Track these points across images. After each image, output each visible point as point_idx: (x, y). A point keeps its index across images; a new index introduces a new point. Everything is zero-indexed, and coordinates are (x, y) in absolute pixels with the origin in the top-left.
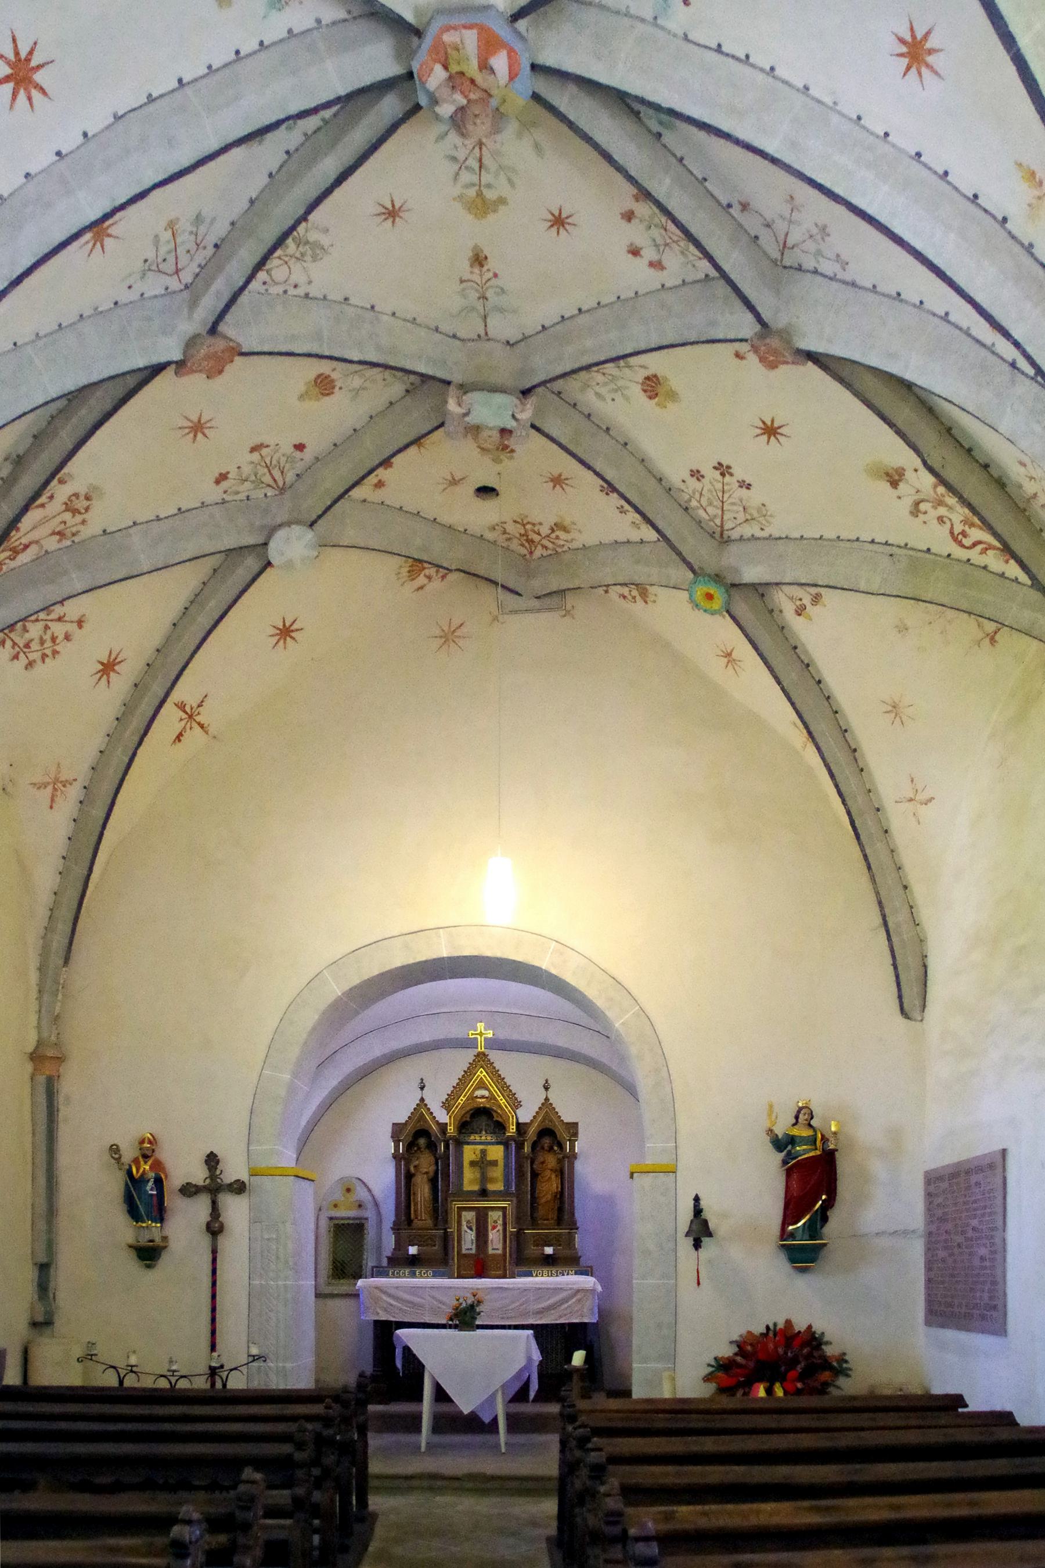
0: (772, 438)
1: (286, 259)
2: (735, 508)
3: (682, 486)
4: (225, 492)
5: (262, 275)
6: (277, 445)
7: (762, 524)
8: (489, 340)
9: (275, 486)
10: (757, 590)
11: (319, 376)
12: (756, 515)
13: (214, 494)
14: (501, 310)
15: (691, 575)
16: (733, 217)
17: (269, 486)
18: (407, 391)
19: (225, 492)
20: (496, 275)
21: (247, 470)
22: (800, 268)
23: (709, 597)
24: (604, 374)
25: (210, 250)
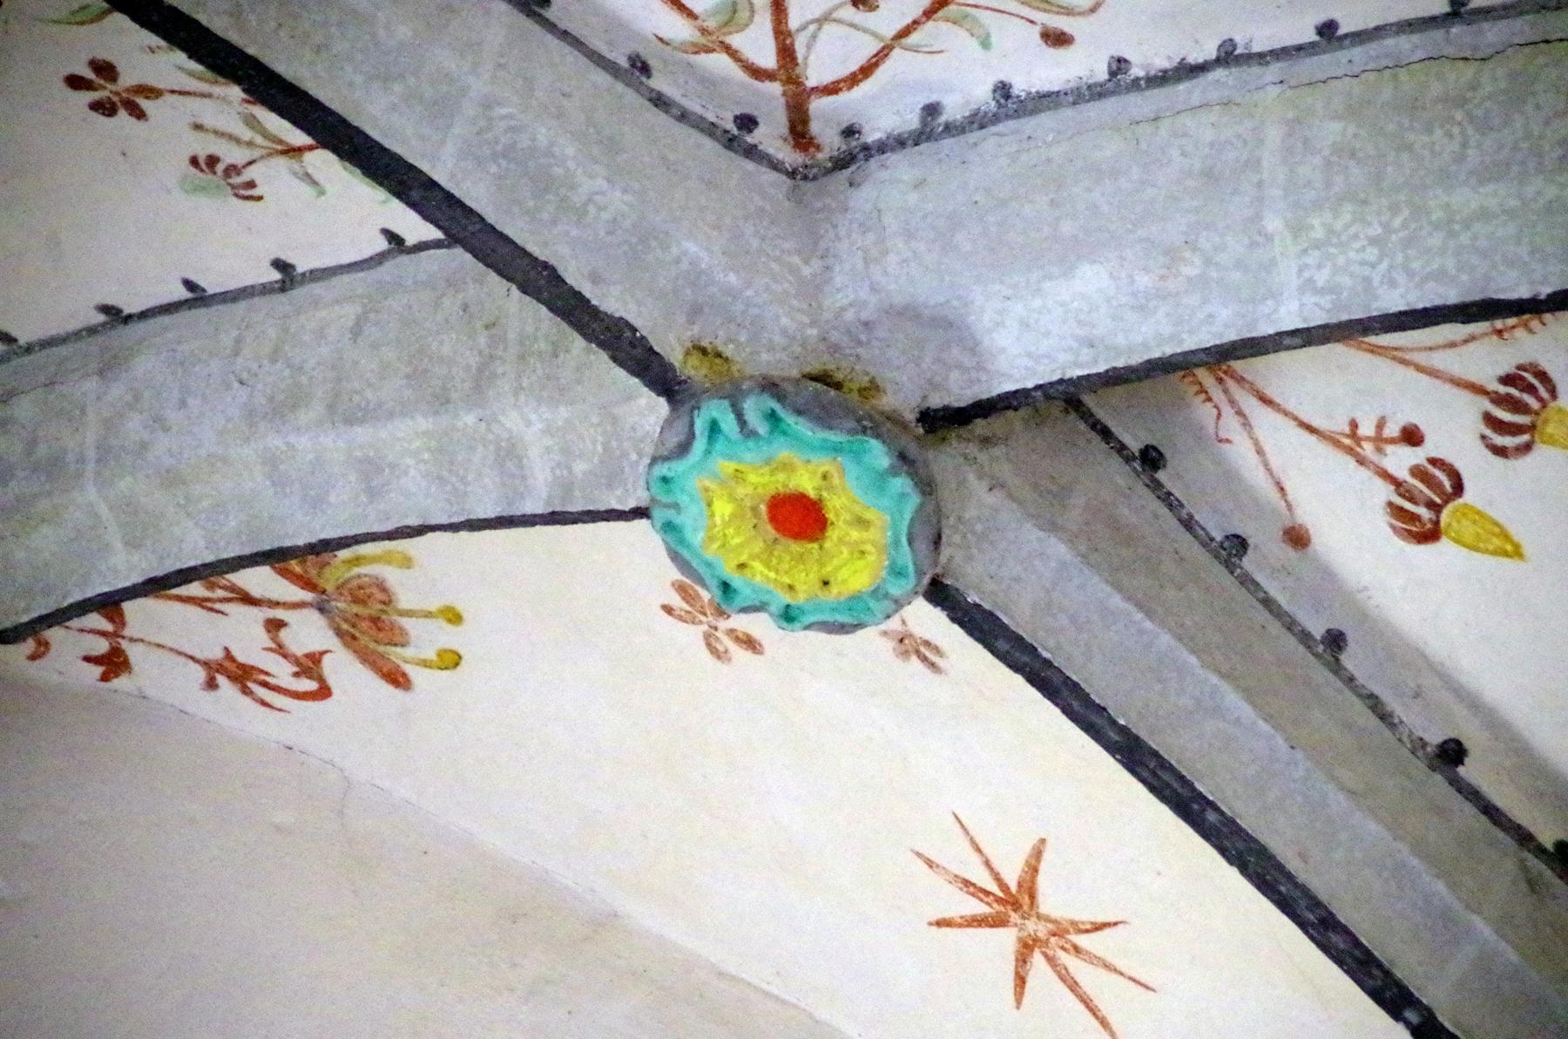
10: (1106, 434)
15: (650, 410)
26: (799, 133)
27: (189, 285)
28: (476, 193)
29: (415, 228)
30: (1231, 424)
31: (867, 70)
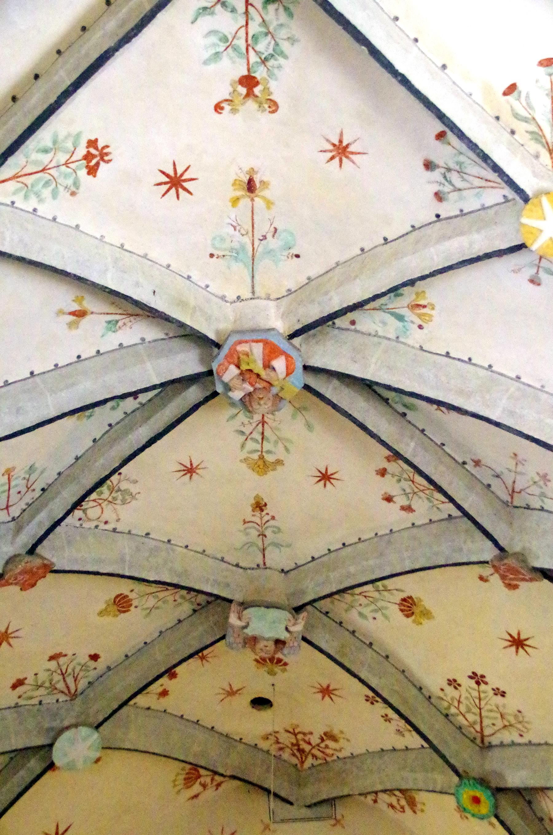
0: (520, 650)
1: (100, 501)
2: (492, 714)
3: (441, 694)
4: (20, 697)
5: (78, 513)
6: (74, 655)
7: (520, 730)
8: (266, 568)
9: (67, 692)
10: (523, 797)
11: (117, 597)
12: (513, 721)
13: (11, 698)
14: (277, 545)
15: (456, 779)
16: (467, 470)
17: (62, 692)
18: (195, 611)
19: (20, 697)
20: (273, 518)
21: (43, 677)
22: (528, 507)
23: (476, 800)
24: (365, 597)
25: (38, 493)
26: (482, 741)
27: (393, 748)
28: (435, 742)
29: (426, 745)
30: (542, 798)
31: (493, 734)
